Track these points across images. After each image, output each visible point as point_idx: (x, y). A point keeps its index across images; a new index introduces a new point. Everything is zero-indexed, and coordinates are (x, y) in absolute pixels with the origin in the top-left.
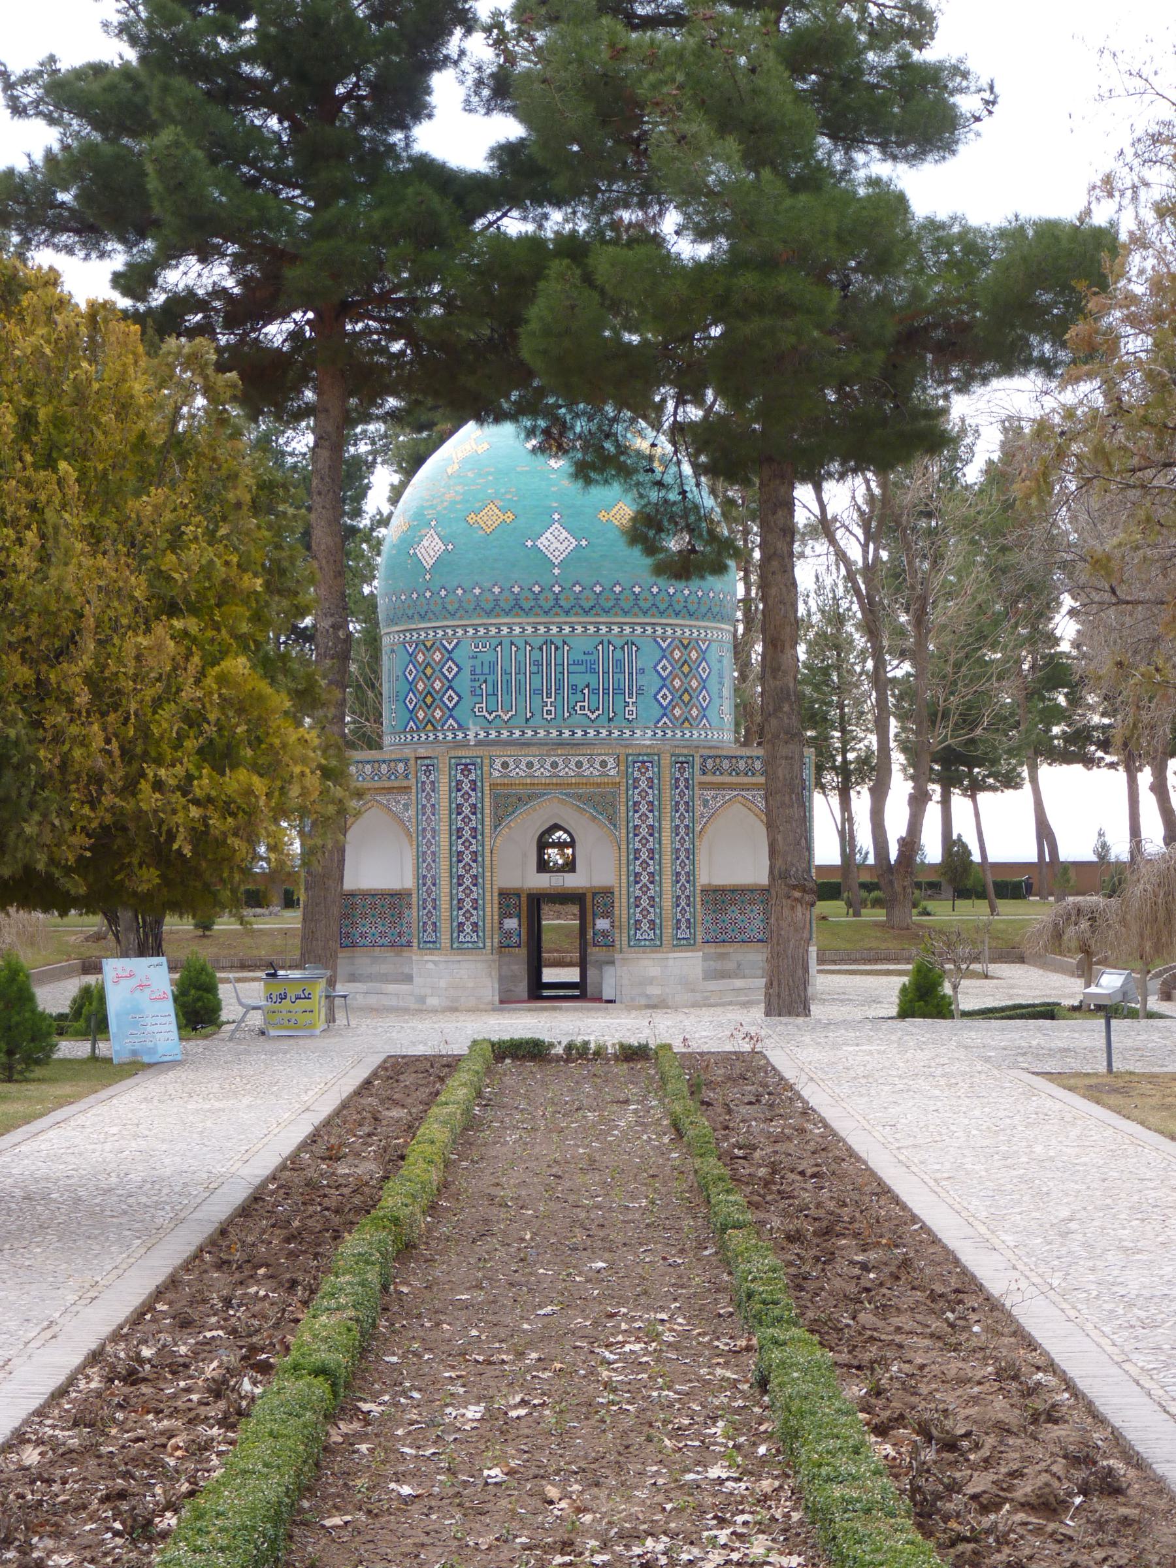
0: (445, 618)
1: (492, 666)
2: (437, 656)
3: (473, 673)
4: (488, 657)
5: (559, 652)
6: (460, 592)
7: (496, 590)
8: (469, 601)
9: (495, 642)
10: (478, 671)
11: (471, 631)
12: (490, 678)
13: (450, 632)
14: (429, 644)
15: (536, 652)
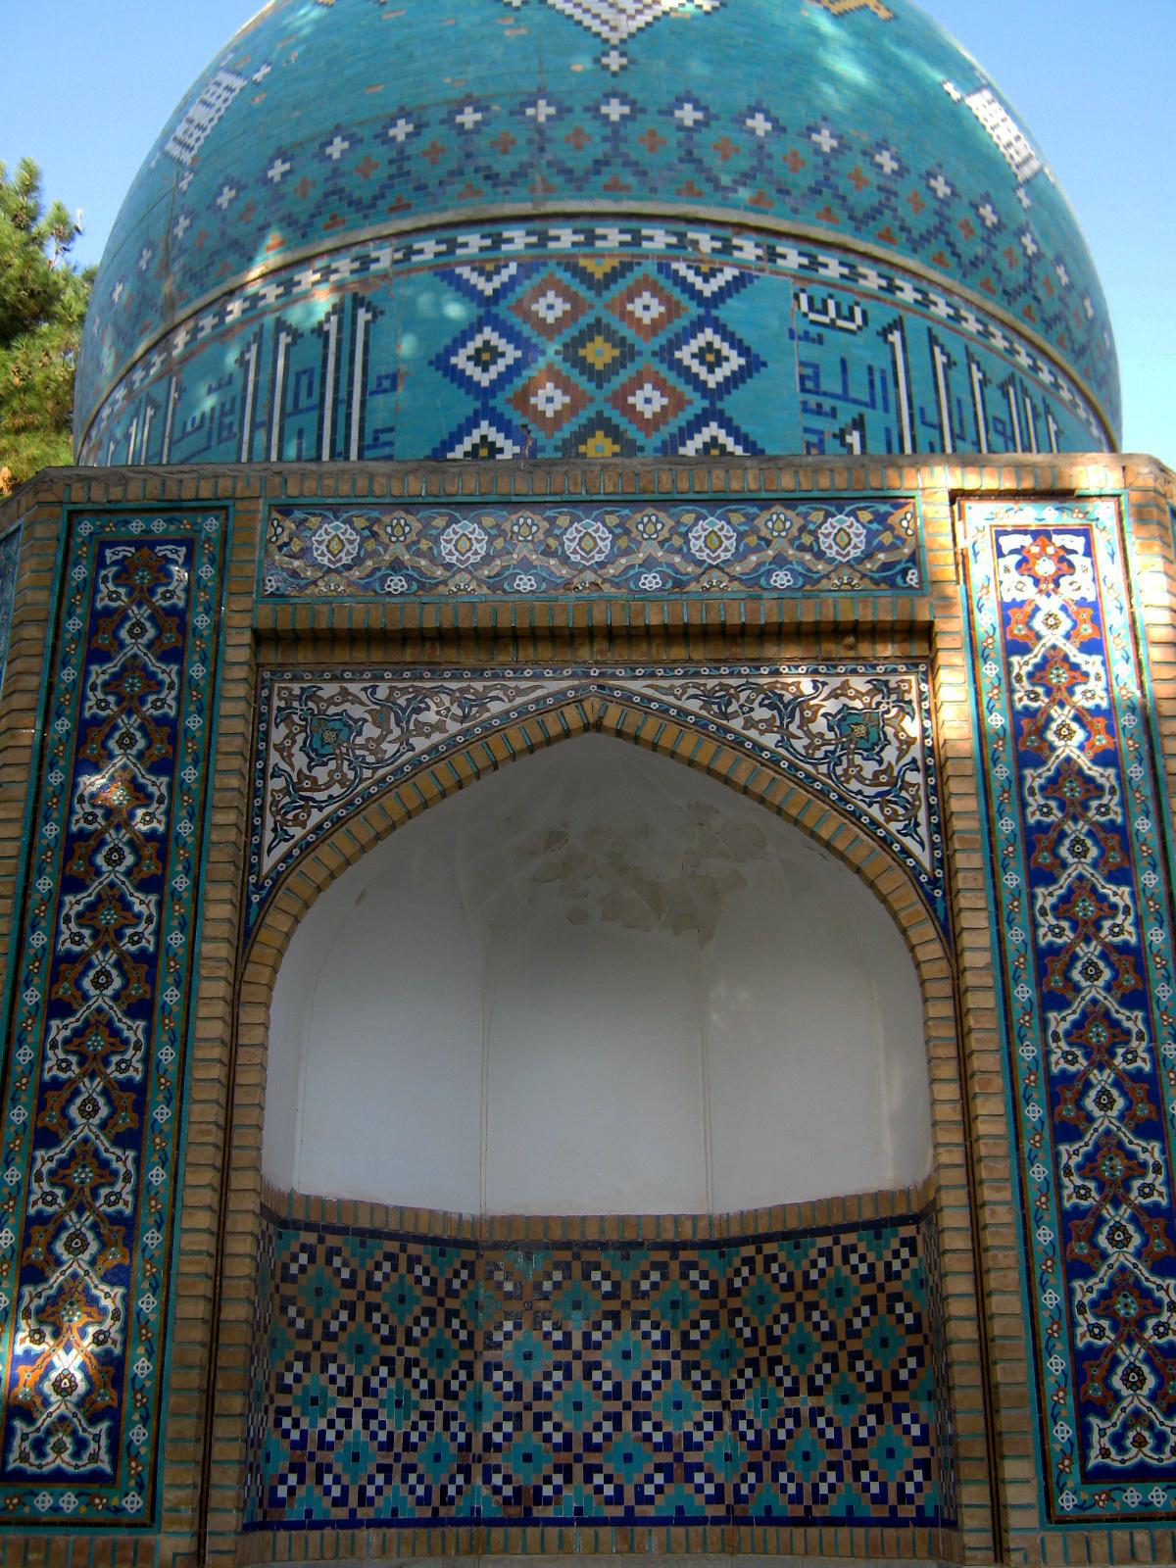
0: (690, 192)
1: (881, 383)
2: (647, 308)
3: (810, 380)
4: (864, 351)
5: (1041, 424)
6: (760, 124)
7: (885, 159)
8: (795, 162)
9: (881, 316)
10: (831, 383)
11: (792, 259)
12: (874, 418)
13: (706, 242)
14: (599, 269)
15: (993, 393)
